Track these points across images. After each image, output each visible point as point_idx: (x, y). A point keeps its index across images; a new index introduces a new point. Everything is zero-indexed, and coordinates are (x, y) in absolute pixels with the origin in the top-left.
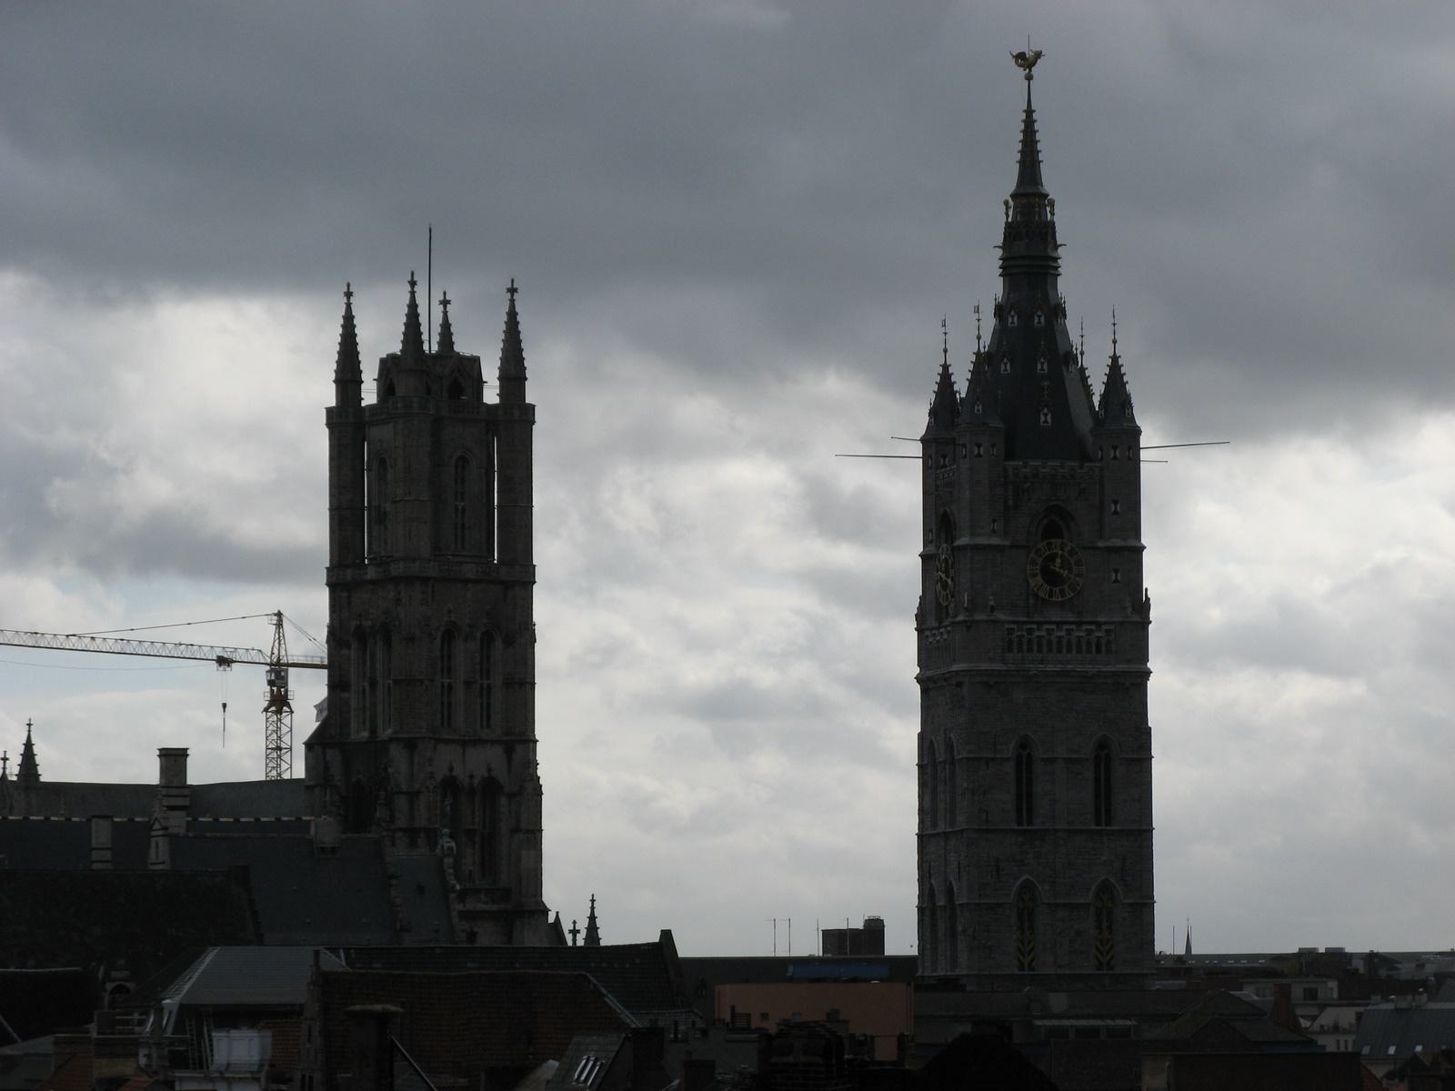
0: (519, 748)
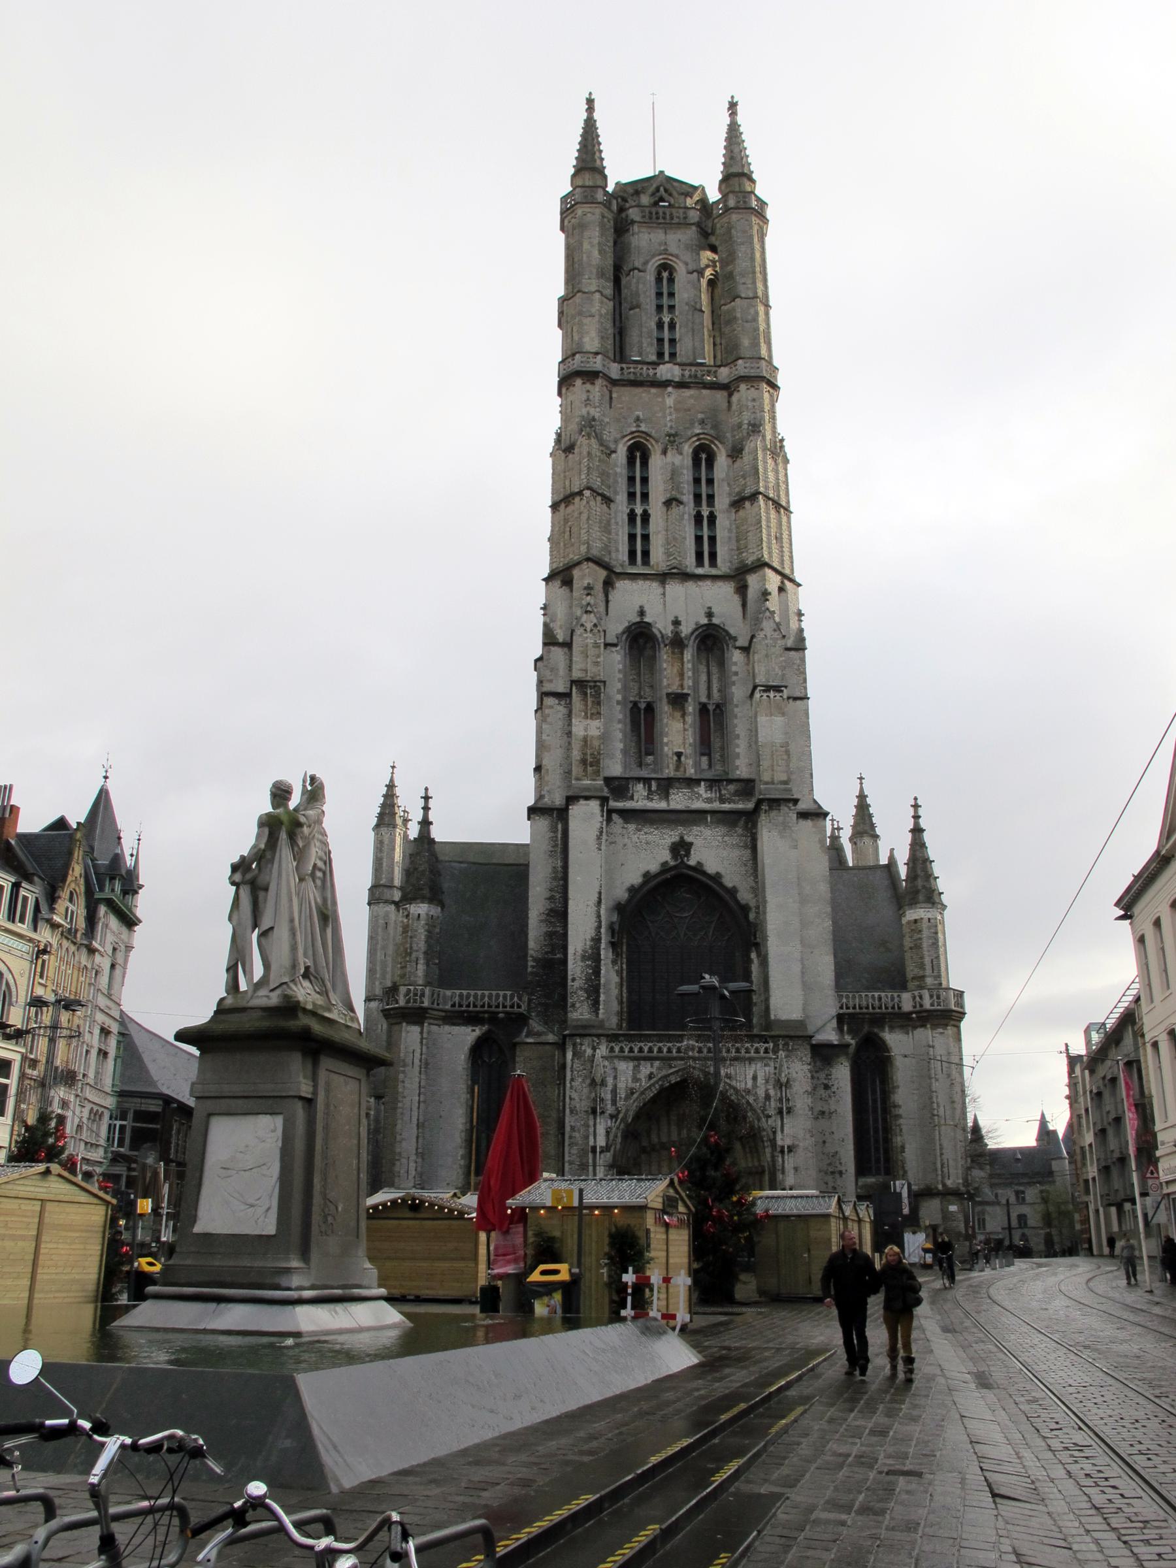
0: (752, 580)
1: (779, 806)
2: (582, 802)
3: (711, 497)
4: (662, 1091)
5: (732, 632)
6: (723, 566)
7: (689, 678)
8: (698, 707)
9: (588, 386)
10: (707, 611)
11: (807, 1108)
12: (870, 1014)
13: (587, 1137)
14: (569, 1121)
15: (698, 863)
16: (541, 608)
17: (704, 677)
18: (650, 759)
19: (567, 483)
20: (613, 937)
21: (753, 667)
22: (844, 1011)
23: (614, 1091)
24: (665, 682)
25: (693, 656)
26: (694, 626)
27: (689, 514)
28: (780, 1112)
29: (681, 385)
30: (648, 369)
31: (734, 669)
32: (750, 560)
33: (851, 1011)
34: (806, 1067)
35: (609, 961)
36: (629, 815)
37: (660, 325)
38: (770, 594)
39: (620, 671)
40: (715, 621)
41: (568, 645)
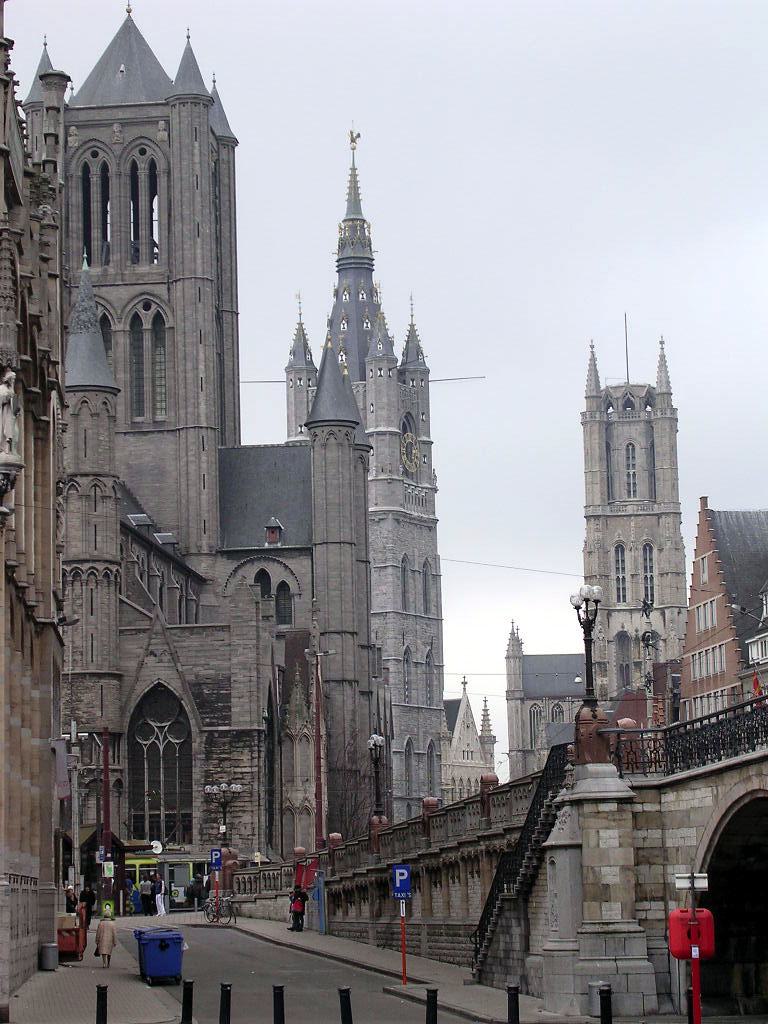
3: (651, 567)
37: (629, 475)
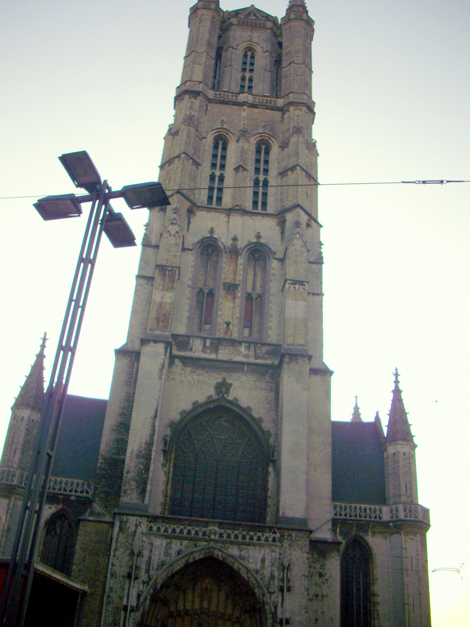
0: (290, 217)
1: (298, 359)
2: (152, 344)
4: (187, 566)
5: (273, 248)
6: (271, 209)
7: (240, 275)
8: (245, 295)
9: (193, 100)
10: (257, 234)
11: (304, 589)
12: (357, 521)
13: (121, 598)
14: (110, 582)
15: (235, 398)
16: (145, 226)
17: (251, 277)
18: (207, 327)
19: (172, 152)
20: (165, 446)
21: (286, 270)
22: (338, 517)
23: (149, 562)
24: (223, 276)
25: (245, 262)
26: (247, 243)
27: (251, 178)
28: (281, 589)
29: (253, 106)
30: (232, 96)
31: (272, 272)
32: (288, 204)
33: (343, 517)
34: (306, 555)
35: (160, 464)
36: (186, 361)
38: (300, 224)
39: (192, 266)
40: (262, 241)
41: (157, 247)
